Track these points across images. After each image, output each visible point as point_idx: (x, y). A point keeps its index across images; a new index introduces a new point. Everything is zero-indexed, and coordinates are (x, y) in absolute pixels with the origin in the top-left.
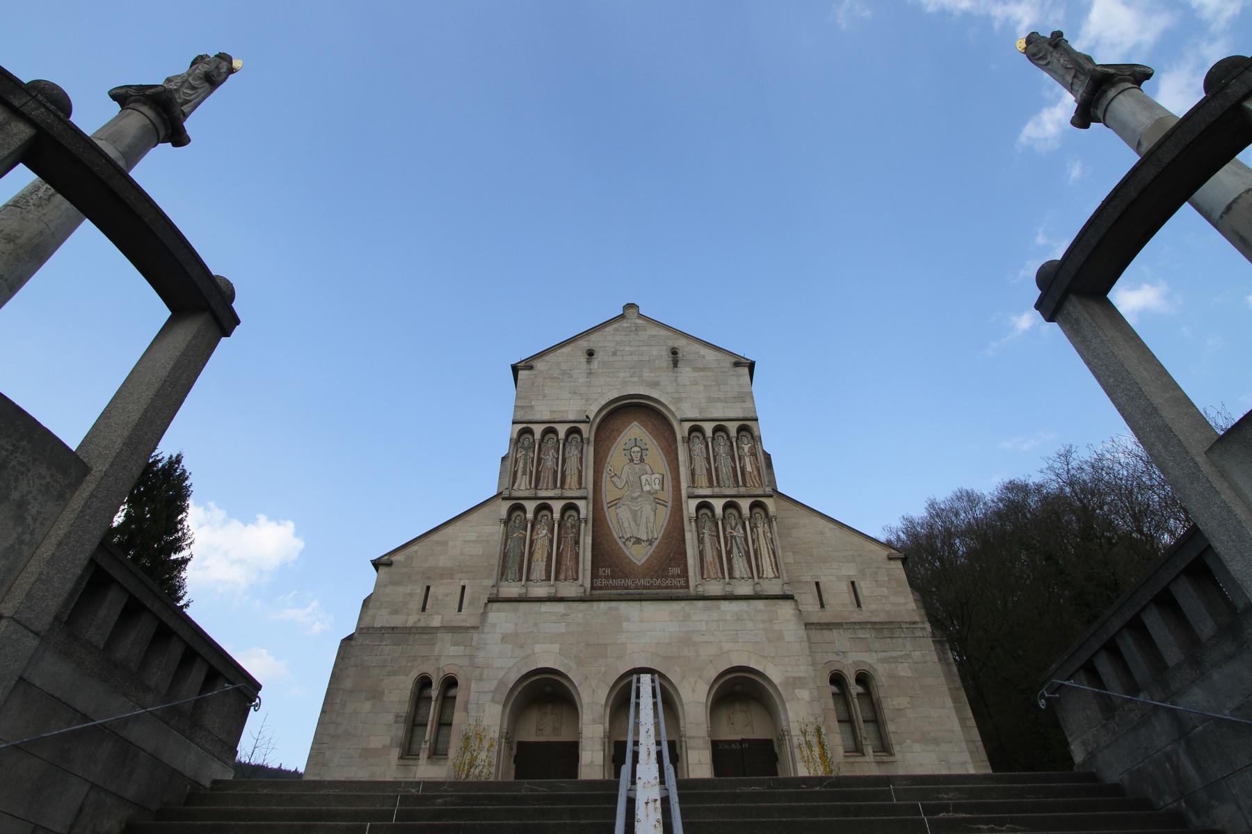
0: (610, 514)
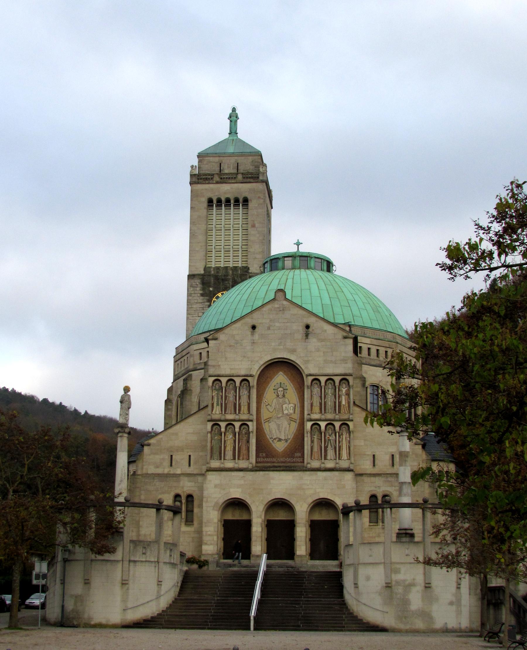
0: (266, 427)
